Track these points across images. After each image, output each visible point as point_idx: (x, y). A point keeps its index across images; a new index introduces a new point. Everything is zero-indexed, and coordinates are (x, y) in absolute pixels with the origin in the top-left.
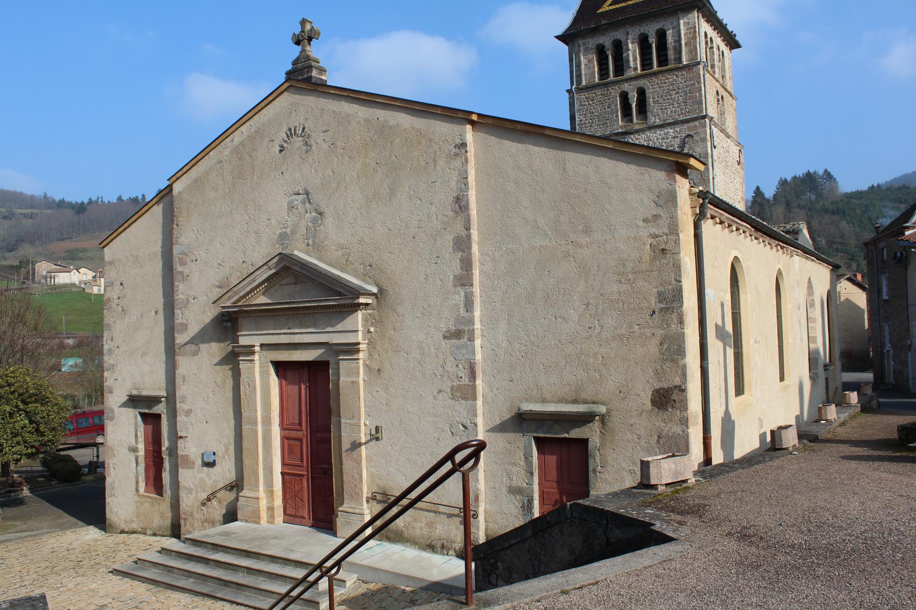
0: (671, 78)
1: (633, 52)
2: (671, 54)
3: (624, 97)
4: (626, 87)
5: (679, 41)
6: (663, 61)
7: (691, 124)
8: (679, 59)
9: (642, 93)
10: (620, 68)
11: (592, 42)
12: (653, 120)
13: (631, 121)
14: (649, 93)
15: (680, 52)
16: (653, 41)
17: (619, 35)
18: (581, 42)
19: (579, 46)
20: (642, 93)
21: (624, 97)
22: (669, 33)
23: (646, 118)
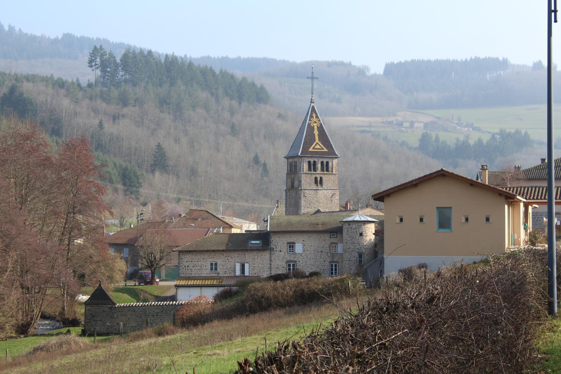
0: (330, 176)
1: (319, 166)
2: (330, 169)
3: (316, 178)
4: (317, 176)
5: (333, 166)
6: (327, 170)
7: (335, 190)
8: (332, 171)
9: (321, 178)
10: (315, 170)
11: (308, 160)
12: (324, 186)
13: (318, 186)
14: (324, 179)
15: (333, 169)
16: (325, 163)
17: (316, 160)
18: (304, 158)
19: (303, 160)
20: (321, 178)
21: (316, 178)
22: (330, 163)
23: (322, 186)
